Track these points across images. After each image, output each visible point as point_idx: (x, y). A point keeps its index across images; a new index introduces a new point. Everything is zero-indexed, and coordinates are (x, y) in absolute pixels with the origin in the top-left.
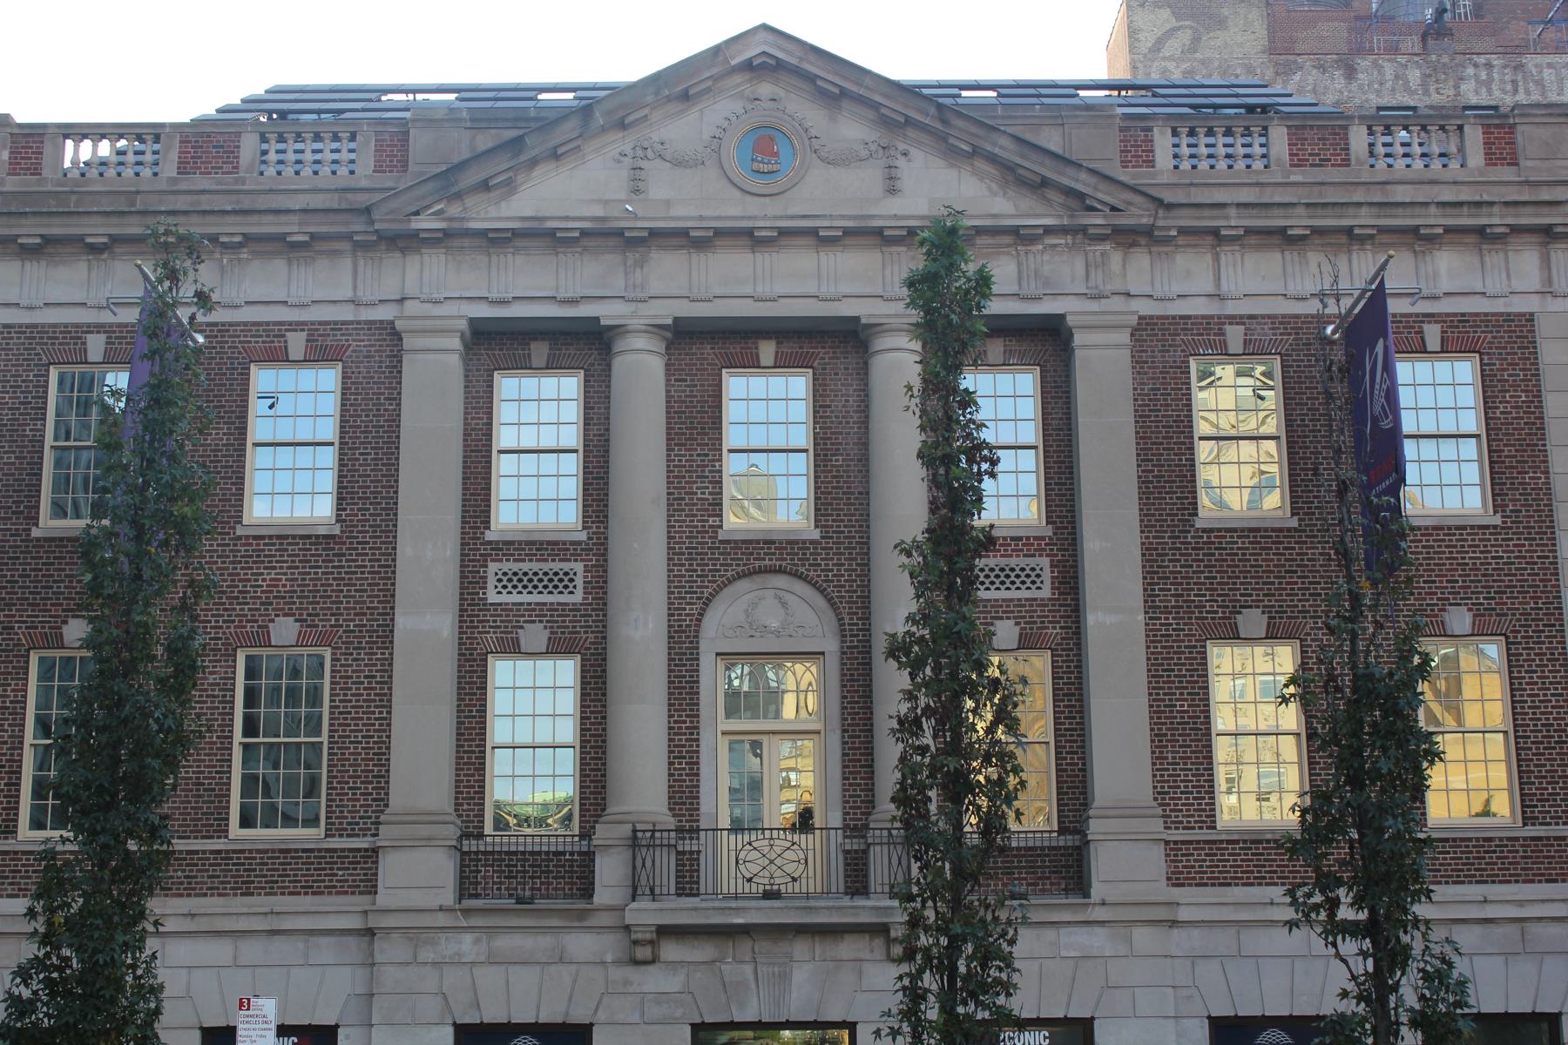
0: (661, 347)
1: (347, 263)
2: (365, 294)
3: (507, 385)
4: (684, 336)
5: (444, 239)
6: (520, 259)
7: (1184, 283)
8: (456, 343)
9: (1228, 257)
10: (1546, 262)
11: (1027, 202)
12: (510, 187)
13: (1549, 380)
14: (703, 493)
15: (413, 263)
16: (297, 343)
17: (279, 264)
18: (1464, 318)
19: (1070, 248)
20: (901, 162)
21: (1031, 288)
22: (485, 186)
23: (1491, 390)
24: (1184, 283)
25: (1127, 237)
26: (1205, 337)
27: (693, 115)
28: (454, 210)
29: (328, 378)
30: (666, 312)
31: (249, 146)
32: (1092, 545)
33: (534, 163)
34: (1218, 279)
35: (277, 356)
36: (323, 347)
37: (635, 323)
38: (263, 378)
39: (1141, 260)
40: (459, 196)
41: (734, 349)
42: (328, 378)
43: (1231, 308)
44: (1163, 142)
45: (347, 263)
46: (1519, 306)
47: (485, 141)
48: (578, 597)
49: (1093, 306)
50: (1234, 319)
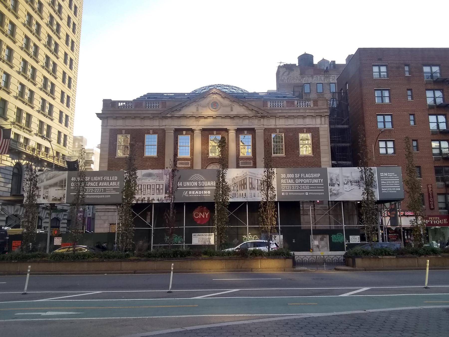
0: (200, 132)
1: (158, 120)
2: (161, 125)
3: (180, 137)
4: (203, 130)
5: (171, 117)
6: (181, 120)
7: (271, 123)
8: (173, 132)
9: (277, 119)
10: (321, 120)
11: (250, 112)
12: (180, 110)
13: (320, 137)
14: (206, 152)
15: (167, 120)
16: (151, 132)
17: (149, 121)
18: (309, 128)
19: (256, 118)
20: (233, 107)
21: (251, 124)
22: (176, 110)
23: (313, 137)
24: (271, 123)
25: (263, 117)
26: (274, 130)
27: (205, 100)
28: (173, 113)
29: (156, 136)
30: (201, 127)
31: (144, 104)
32: (258, 159)
33: (183, 107)
34: (276, 122)
35: (149, 133)
36: (155, 132)
37: (197, 129)
38: (147, 136)
39: (265, 120)
40: (173, 111)
41: (210, 132)
42: (156, 136)
43: (278, 127)
44: (269, 104)
45: (158, 120)
46: (317, 126)
47: (177, 104)
48: (189, 166)
49: (259, 127)
50: (278, 128)
